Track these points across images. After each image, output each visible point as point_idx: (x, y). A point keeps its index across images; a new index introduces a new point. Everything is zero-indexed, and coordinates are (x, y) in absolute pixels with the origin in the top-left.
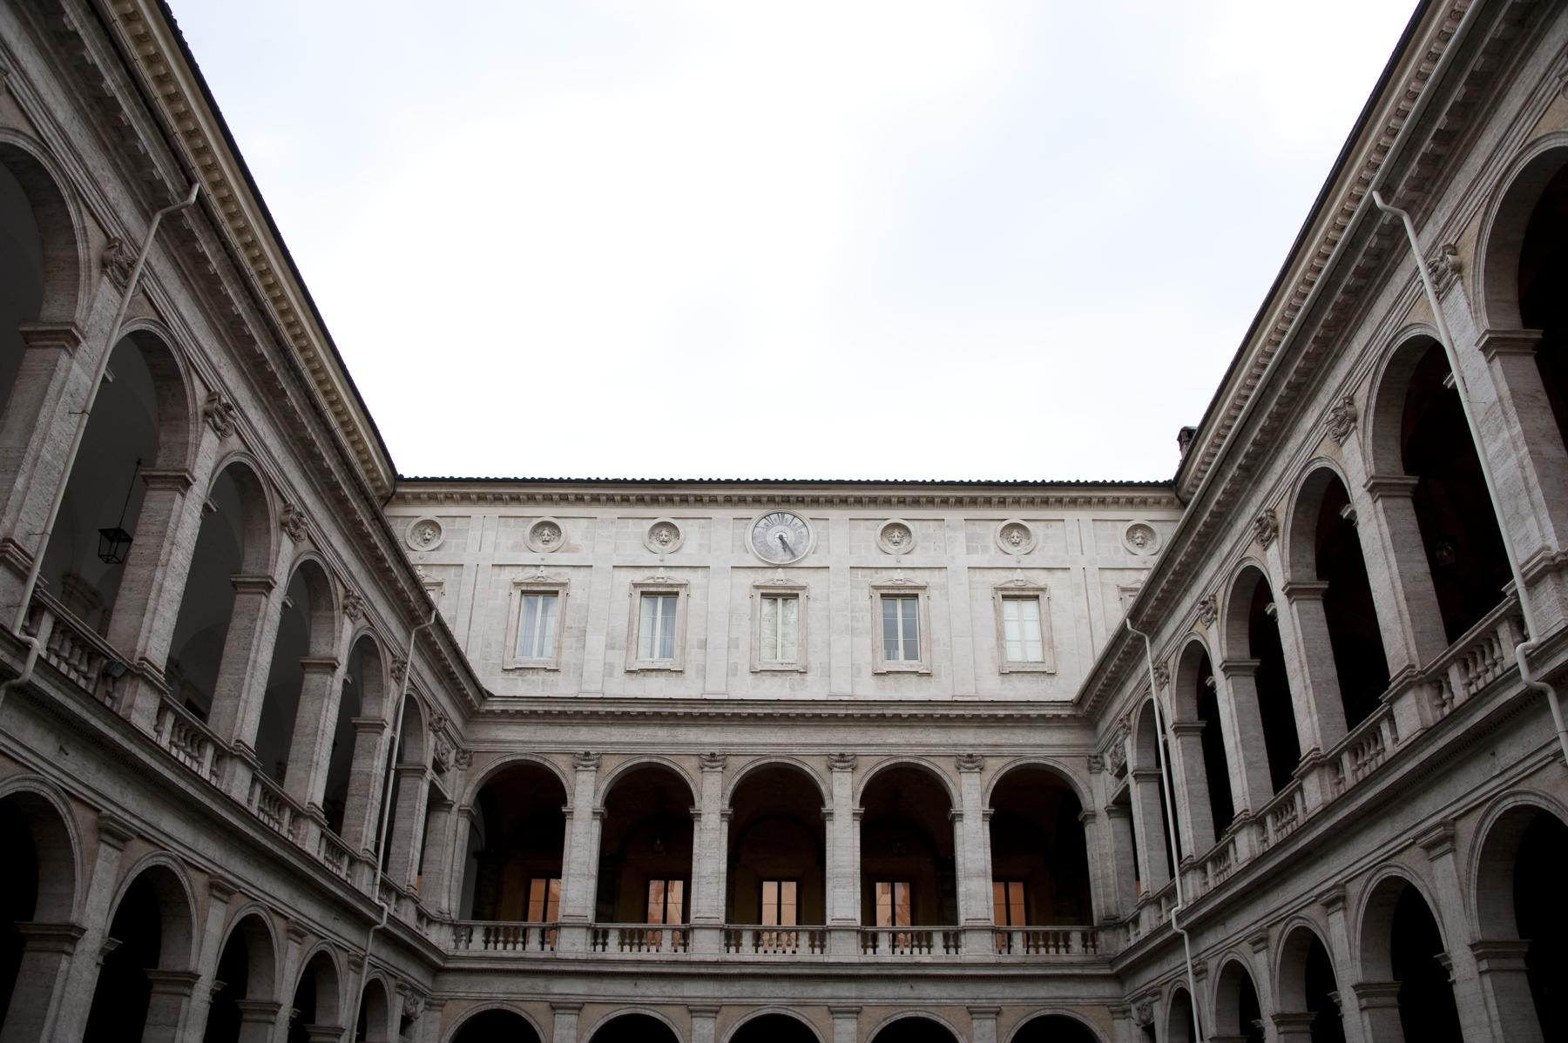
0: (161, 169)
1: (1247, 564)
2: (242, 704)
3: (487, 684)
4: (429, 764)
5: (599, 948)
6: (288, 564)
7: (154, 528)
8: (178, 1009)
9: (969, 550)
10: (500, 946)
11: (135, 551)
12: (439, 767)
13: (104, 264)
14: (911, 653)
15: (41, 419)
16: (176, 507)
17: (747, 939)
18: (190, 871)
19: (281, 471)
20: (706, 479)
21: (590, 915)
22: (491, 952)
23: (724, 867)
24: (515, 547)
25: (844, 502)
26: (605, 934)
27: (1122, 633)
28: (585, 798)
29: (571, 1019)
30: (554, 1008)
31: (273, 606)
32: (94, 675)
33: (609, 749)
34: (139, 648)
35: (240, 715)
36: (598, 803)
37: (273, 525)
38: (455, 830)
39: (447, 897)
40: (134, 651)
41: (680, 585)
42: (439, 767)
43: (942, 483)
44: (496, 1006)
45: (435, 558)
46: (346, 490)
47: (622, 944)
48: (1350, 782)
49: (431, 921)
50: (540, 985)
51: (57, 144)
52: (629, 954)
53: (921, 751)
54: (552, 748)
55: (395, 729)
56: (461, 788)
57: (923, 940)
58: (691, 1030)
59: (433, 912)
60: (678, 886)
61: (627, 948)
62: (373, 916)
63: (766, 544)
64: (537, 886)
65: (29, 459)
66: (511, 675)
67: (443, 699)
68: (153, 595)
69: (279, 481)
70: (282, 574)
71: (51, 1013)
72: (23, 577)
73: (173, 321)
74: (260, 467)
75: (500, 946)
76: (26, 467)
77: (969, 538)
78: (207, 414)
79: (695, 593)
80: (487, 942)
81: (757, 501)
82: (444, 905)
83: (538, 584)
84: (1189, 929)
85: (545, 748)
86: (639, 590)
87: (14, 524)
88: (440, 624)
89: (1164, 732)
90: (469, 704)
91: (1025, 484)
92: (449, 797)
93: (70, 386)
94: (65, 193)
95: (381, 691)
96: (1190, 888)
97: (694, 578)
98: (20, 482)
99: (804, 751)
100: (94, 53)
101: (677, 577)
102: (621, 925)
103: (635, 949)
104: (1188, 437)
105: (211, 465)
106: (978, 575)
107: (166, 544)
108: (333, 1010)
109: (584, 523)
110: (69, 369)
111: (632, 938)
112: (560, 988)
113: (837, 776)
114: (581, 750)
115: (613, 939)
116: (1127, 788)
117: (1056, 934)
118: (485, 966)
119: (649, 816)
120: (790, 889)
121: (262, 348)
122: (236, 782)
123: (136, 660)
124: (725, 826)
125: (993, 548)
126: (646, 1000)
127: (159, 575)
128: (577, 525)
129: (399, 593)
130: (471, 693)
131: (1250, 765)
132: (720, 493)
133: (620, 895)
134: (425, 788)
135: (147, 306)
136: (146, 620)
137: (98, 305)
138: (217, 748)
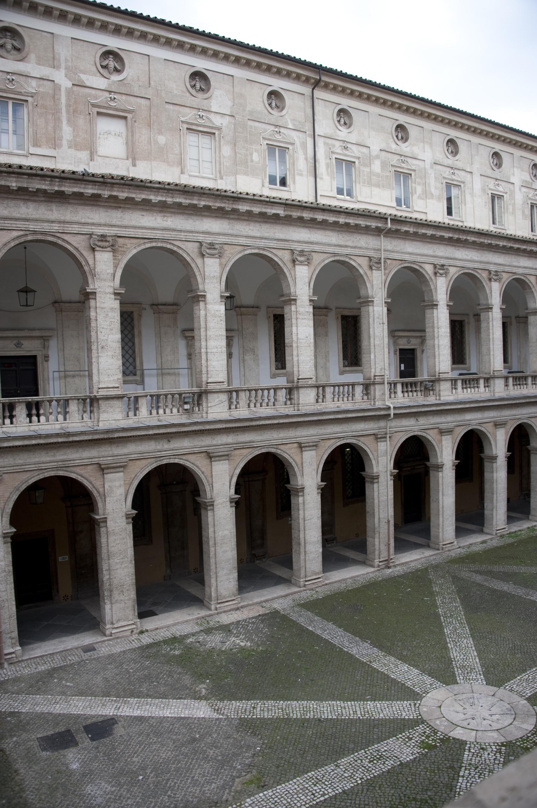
0: (373, 224)
2: (492, 357)
6: (498, 292)
7: (431, 325)
8: (492, 467)
11: (427, 334)
13: (371, 268)
15: (371, 333)
16: (435, 315)
34: (437, 370)
35: (492, 361)
65: (372, 347)
68: (437, 350)
71: (441, 488)
74: (469, 269)
76: (372, 350)
78: (435, 274)
93: (376, 315)
94: (347, 260)
98: (372, 356)
100: (331, 219)
105: (445, 289)
107: (436, 330)
121: (447, 235)
123: (437, 374)
127: (436, 342)
135: (394, 262)
136: (437, 360)
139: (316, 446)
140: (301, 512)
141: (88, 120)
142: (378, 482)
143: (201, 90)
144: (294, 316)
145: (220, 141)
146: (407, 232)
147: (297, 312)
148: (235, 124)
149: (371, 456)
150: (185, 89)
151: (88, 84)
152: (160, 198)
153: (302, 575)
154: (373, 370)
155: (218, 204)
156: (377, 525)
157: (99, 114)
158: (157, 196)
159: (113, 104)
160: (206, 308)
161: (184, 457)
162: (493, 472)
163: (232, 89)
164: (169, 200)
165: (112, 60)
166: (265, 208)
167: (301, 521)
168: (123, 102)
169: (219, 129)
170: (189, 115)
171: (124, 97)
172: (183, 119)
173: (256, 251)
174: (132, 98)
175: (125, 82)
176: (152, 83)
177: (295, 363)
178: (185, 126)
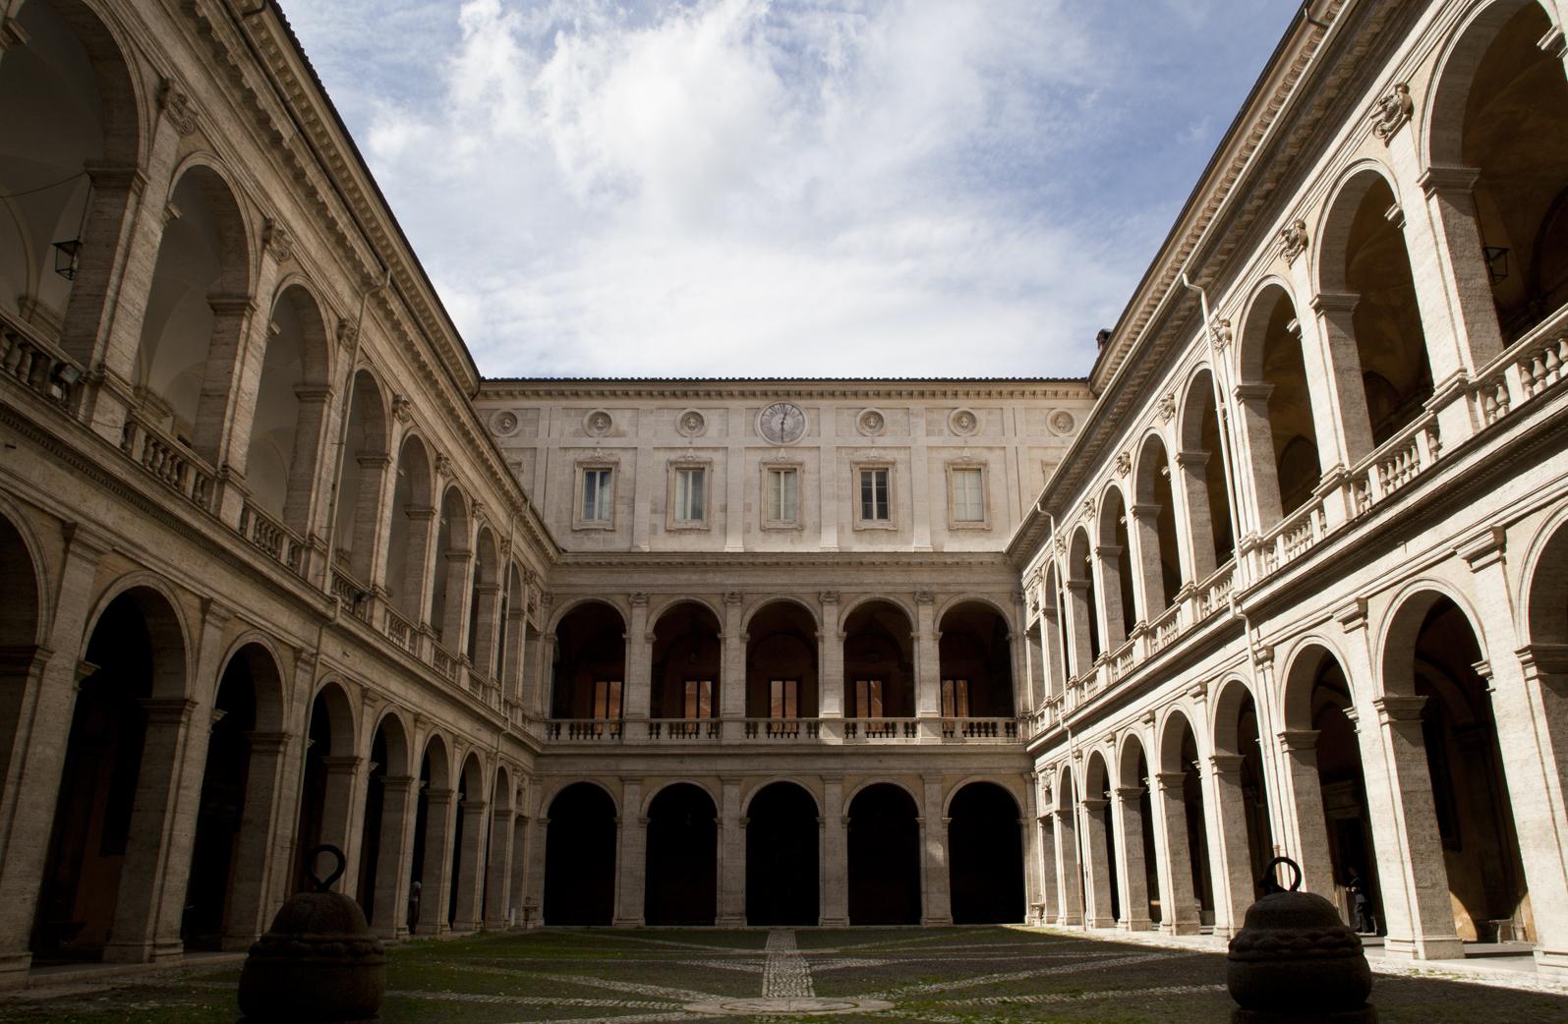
1: (1112, 483)
3: (561, 544)
4: (526, 610)
5: (654, 736)
9: (929, 434)
10: (581, 737)
12: (531, 609)
13: (339, 338)
14: (883, 513)
16: (383, 480)
17: (762, 729)
18: (405, 713)
19: (435, 433)
20: (724, 378)
21: (647, 713)
22: (575, 741)
23: (743, 677)
24: (576, 434)
25: (833, 394)
26: (658, 726)
27: (1035, 514)
28: (640, 628)
29: (636, 788)
30: (622, 780)
31: (435, 525)
32: (352, 602)
33: (656, 590)
36: (650, 629)
37: (432, 470)
38: (545, 651)
39: (542, 705)
40: (369, 581)
41: (705, 463)
42: (531, 609)
43: (908, 380)
44: (581, 780)
45: (514, 443)
46: (474, 434)
47: (671, 734)
48: (1161, 646)
49: (531, 721)
50: (612, 763)
51: (313, 274)
52: (676, 740)
53: (889, 589)
54: (614, 590)
55: (505, 590)
56: (546, 622)
57: (889, 729)
58: (723, 794)
59: (531, 714)
60: (708, 684)
61: (674, 736)
62: (500, 725)
63: (770, 429)
64: (601, 687)
66: (579, 535)
67: (533, 559)
69: (433, 440)
70: (438, 504)
72: (323, 555)
73: (374, 357)
75: (581, 737)
76: (315, 486)
77: (929, 423)
78: (395, 411)
79: (718, 469)
80: (571, 734)
81: (765, 394)
82: (538, 708)
83: (595, 463)
84: (1071, 727)
85: (608, 590)
86: (674, 468)
87: (313, 523)
88: (533, 511)
89: (1061, 586)
90: (550, 559)
91: (973, 380)
92: (537, 628)
93: (331, 426)
94: (318, 300)
95: (494, 564)
96: (1072, 700)
97: (717, 457)
98: (313, 495)
99: (802, 590)
100: (334, 209)
101: (704, 456)
102: (670, 720)
103: (681, 736)
104: (1105, 338)
105: (398, 444)
106: (934, 454)
107: (380, 507)
108: (479, 791)
109: (628, 414)
110: (329, 415)
111: (678, 729)
112: (627, 766)
113: (827, 608)
114: (634, 591)
115: (664, 731)
116: (1038, 620)
117: (986, 725)
118: (571, 751)
119: (688, 637)
120: (792, 686)
122: (424, 651)
124: (744, 647)
125: (946, 431)
126: (689, 773)
128: (623, 415)
129: (506, 493)
130: (551, 551)
131: (1110, 620)
132: (736, 388)
133: (666, 699)
134: (524, 626)
137: (339, 367)
138: (412, 629)
139: (225, 620)
140: (176, 765)
142: (285, 754)
144: (242, 342)
146: (389, 314)
147: (248, 336)
149: (284, 693)
153: (150, 929)
154: (310, 524)
156: (269, 850)
160: (137, 212)
161: (24, 509)
162: (402, 810)
167: (173, 786)
173: (225, 176)
177: (226, 432)
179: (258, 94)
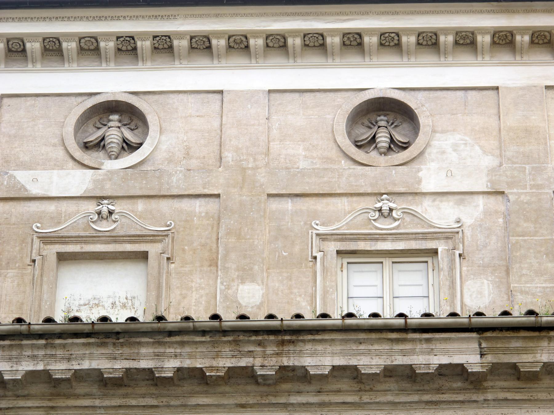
141: (28, 279)
143: (395, 146)
145: (452, 269)
148: (507, 216)
150: (334, 153)
151: (35, 190)
152: (27, 366)
155: (226, 362)
157: (62, 258)
158: (18, 360)
159: (105, 227)
163: (493, 122)
164: (59, 368)
165: (116, 121)
166: (404, 353)
168: (134, 217)
169: (448, 236)
170: (345, 215)
171: (140, 205)
172: (322, 230)
174: (165, 205)
175: (145, 168)
176: (229, 156)
178: (333, 247)
179: (353, 362)
